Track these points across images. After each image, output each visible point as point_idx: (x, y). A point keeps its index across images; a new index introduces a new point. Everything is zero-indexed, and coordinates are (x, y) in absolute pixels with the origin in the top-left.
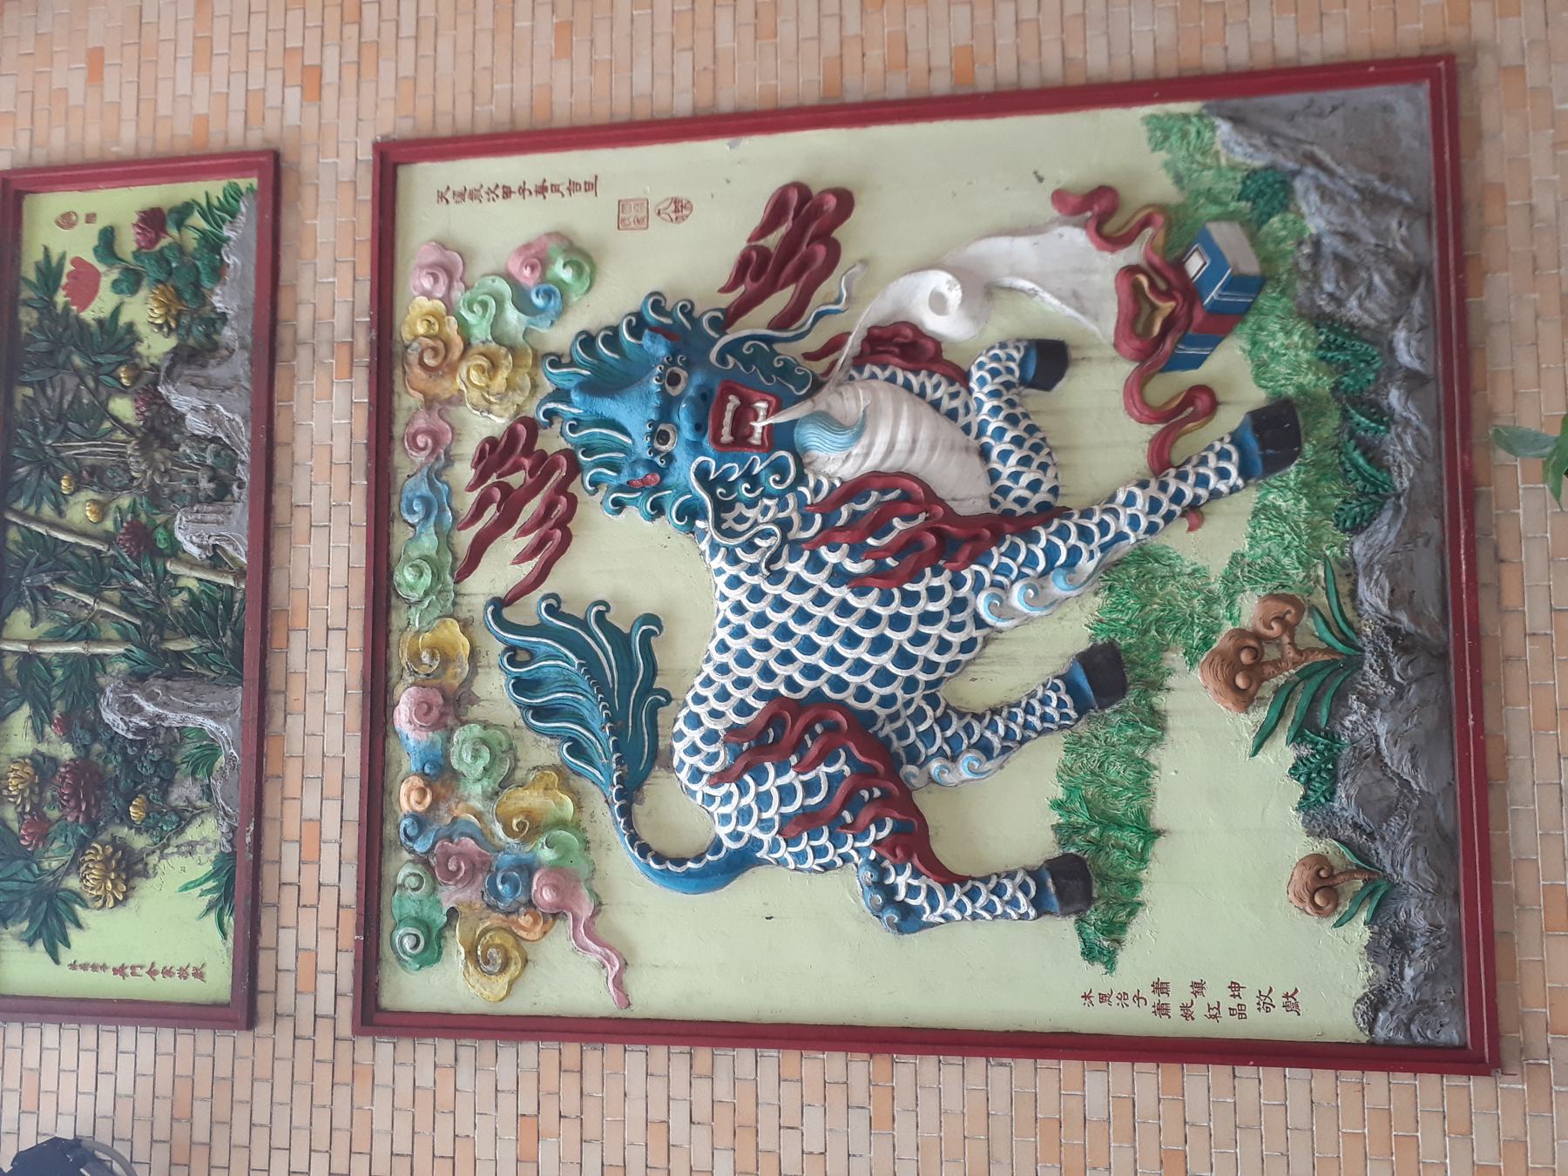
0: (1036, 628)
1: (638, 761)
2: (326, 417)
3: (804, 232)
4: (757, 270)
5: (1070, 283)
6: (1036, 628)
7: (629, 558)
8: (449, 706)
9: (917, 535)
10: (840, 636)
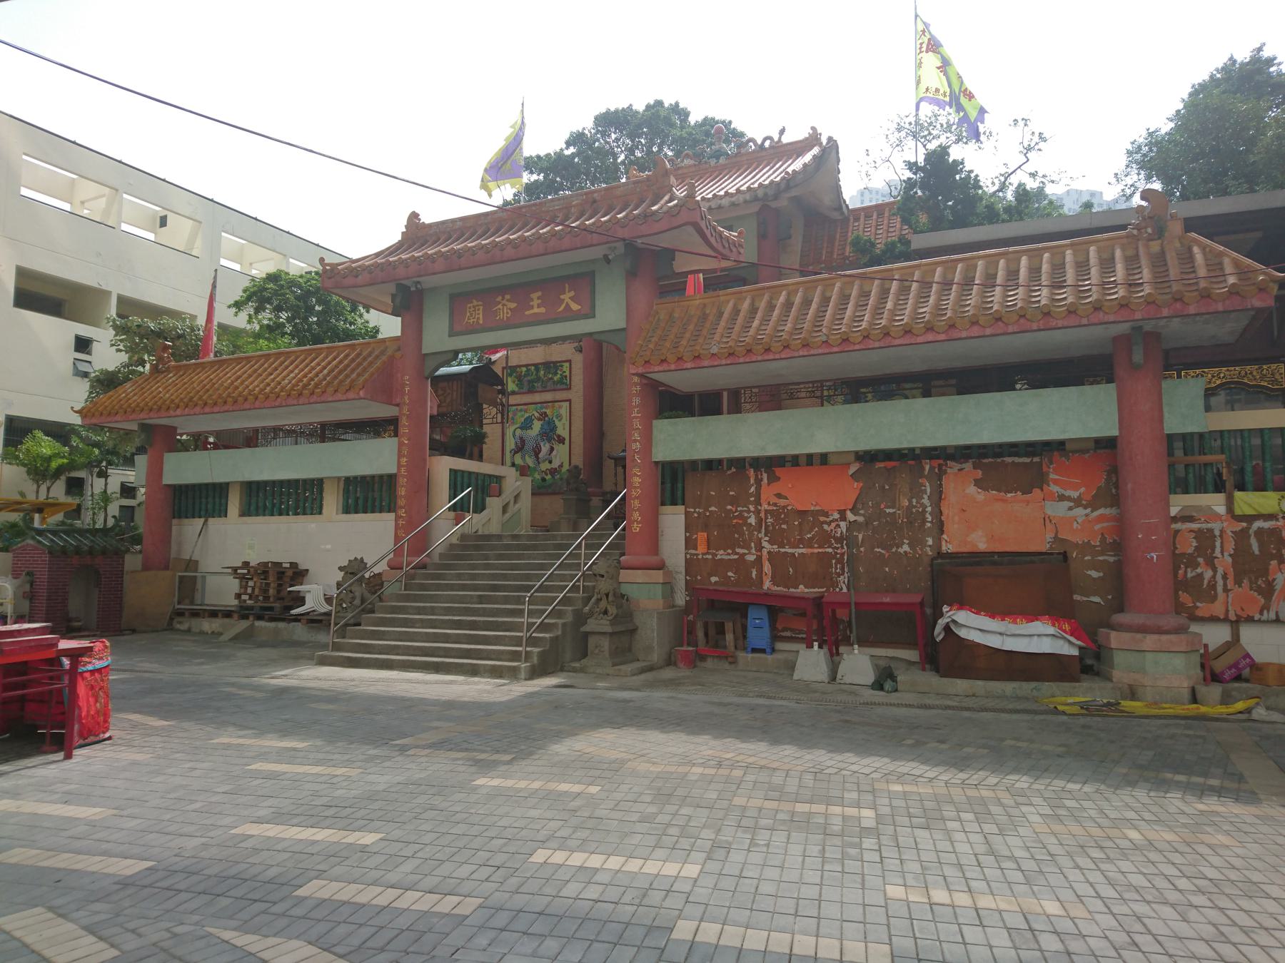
0: (530, 461)
1: (521, 428)
2: (548, 396)
3: (561, 440)
4: (559, 436)
5: (555, 464)
6: (530, 461)
7: (537, 426)
8: (526, 411)
9: (537, 451)
10: (530, 445)
